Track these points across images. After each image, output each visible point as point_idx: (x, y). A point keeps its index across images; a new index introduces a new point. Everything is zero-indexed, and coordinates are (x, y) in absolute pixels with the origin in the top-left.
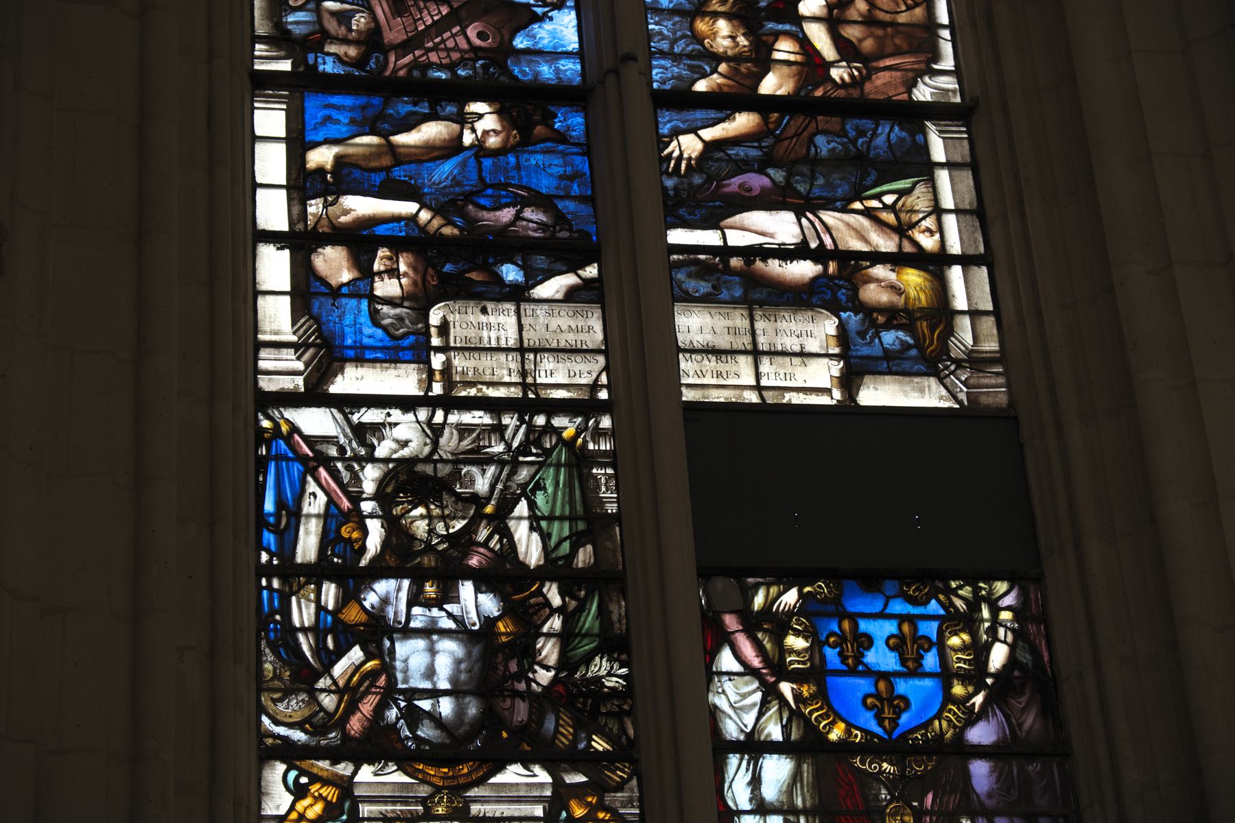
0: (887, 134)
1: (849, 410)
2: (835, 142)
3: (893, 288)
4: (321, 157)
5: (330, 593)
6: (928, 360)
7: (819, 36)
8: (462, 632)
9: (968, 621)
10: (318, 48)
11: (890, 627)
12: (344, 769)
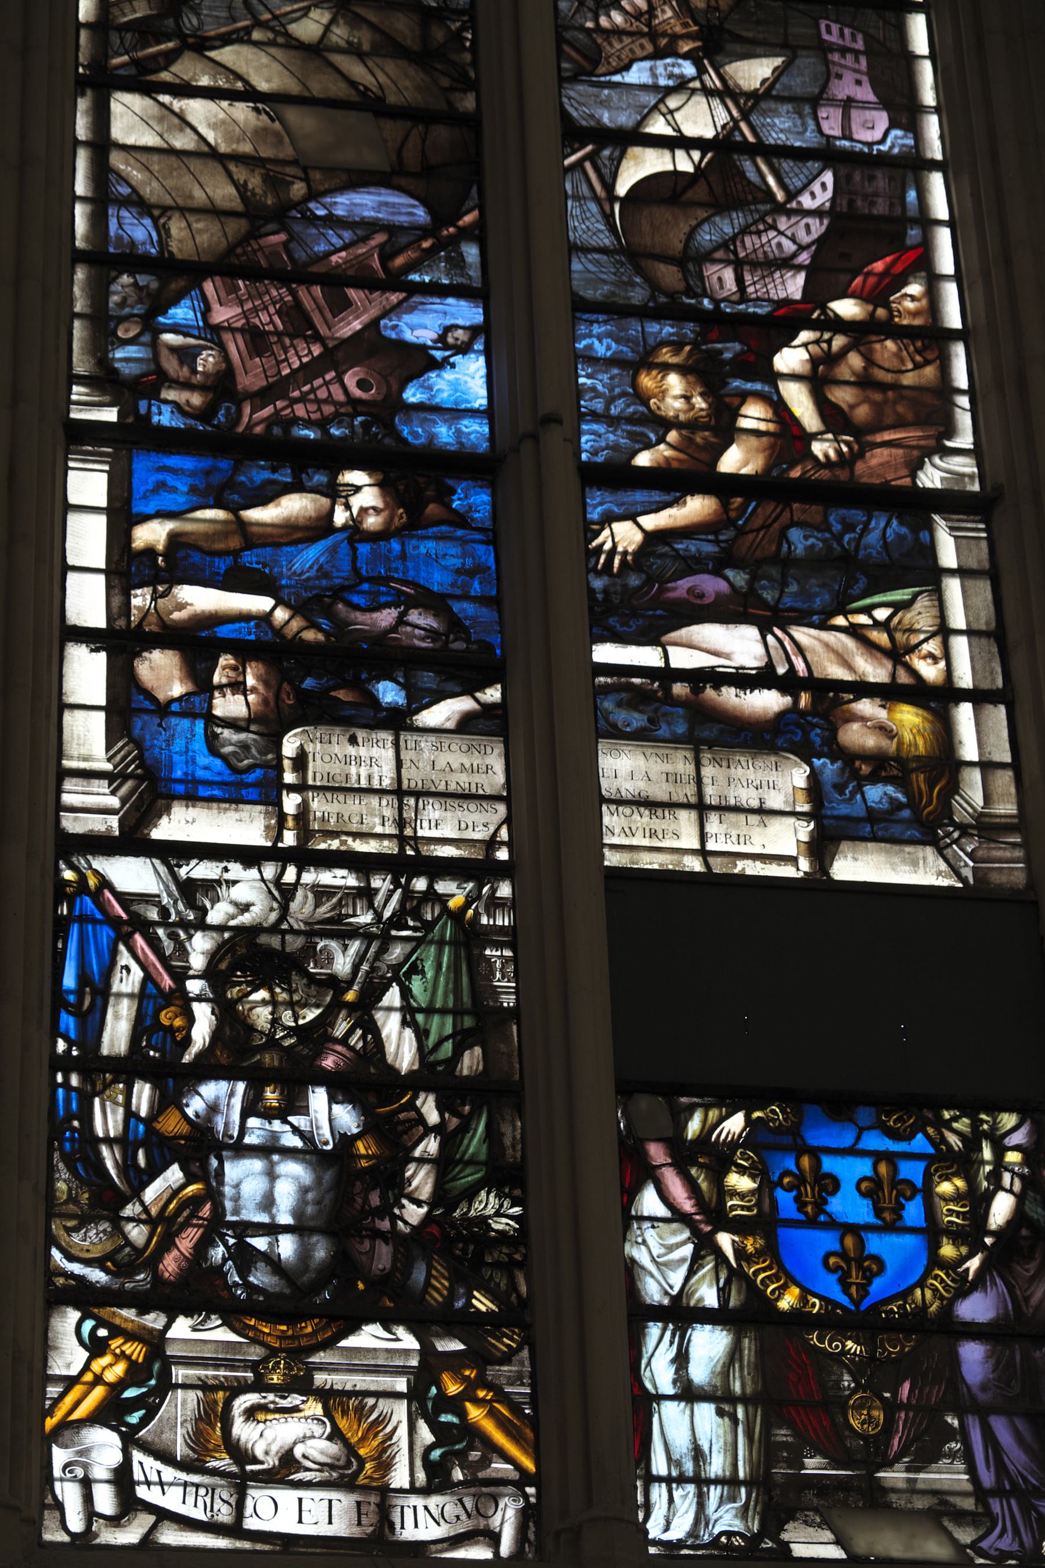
0: (882, 530)
1: (820, 886)
2: (814, 538)
3: (883, 729)
4: (152, 534)
5: (143, 1095)
6: (924, 824)
7: (799, 400)
8: (309, 1151)
9: (964, 1163)
10: (153, 394)
11: (863, 1167)
12: (154, 1320)
